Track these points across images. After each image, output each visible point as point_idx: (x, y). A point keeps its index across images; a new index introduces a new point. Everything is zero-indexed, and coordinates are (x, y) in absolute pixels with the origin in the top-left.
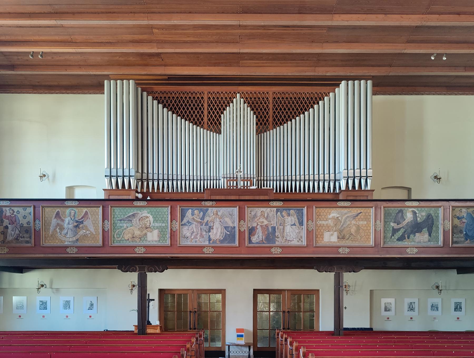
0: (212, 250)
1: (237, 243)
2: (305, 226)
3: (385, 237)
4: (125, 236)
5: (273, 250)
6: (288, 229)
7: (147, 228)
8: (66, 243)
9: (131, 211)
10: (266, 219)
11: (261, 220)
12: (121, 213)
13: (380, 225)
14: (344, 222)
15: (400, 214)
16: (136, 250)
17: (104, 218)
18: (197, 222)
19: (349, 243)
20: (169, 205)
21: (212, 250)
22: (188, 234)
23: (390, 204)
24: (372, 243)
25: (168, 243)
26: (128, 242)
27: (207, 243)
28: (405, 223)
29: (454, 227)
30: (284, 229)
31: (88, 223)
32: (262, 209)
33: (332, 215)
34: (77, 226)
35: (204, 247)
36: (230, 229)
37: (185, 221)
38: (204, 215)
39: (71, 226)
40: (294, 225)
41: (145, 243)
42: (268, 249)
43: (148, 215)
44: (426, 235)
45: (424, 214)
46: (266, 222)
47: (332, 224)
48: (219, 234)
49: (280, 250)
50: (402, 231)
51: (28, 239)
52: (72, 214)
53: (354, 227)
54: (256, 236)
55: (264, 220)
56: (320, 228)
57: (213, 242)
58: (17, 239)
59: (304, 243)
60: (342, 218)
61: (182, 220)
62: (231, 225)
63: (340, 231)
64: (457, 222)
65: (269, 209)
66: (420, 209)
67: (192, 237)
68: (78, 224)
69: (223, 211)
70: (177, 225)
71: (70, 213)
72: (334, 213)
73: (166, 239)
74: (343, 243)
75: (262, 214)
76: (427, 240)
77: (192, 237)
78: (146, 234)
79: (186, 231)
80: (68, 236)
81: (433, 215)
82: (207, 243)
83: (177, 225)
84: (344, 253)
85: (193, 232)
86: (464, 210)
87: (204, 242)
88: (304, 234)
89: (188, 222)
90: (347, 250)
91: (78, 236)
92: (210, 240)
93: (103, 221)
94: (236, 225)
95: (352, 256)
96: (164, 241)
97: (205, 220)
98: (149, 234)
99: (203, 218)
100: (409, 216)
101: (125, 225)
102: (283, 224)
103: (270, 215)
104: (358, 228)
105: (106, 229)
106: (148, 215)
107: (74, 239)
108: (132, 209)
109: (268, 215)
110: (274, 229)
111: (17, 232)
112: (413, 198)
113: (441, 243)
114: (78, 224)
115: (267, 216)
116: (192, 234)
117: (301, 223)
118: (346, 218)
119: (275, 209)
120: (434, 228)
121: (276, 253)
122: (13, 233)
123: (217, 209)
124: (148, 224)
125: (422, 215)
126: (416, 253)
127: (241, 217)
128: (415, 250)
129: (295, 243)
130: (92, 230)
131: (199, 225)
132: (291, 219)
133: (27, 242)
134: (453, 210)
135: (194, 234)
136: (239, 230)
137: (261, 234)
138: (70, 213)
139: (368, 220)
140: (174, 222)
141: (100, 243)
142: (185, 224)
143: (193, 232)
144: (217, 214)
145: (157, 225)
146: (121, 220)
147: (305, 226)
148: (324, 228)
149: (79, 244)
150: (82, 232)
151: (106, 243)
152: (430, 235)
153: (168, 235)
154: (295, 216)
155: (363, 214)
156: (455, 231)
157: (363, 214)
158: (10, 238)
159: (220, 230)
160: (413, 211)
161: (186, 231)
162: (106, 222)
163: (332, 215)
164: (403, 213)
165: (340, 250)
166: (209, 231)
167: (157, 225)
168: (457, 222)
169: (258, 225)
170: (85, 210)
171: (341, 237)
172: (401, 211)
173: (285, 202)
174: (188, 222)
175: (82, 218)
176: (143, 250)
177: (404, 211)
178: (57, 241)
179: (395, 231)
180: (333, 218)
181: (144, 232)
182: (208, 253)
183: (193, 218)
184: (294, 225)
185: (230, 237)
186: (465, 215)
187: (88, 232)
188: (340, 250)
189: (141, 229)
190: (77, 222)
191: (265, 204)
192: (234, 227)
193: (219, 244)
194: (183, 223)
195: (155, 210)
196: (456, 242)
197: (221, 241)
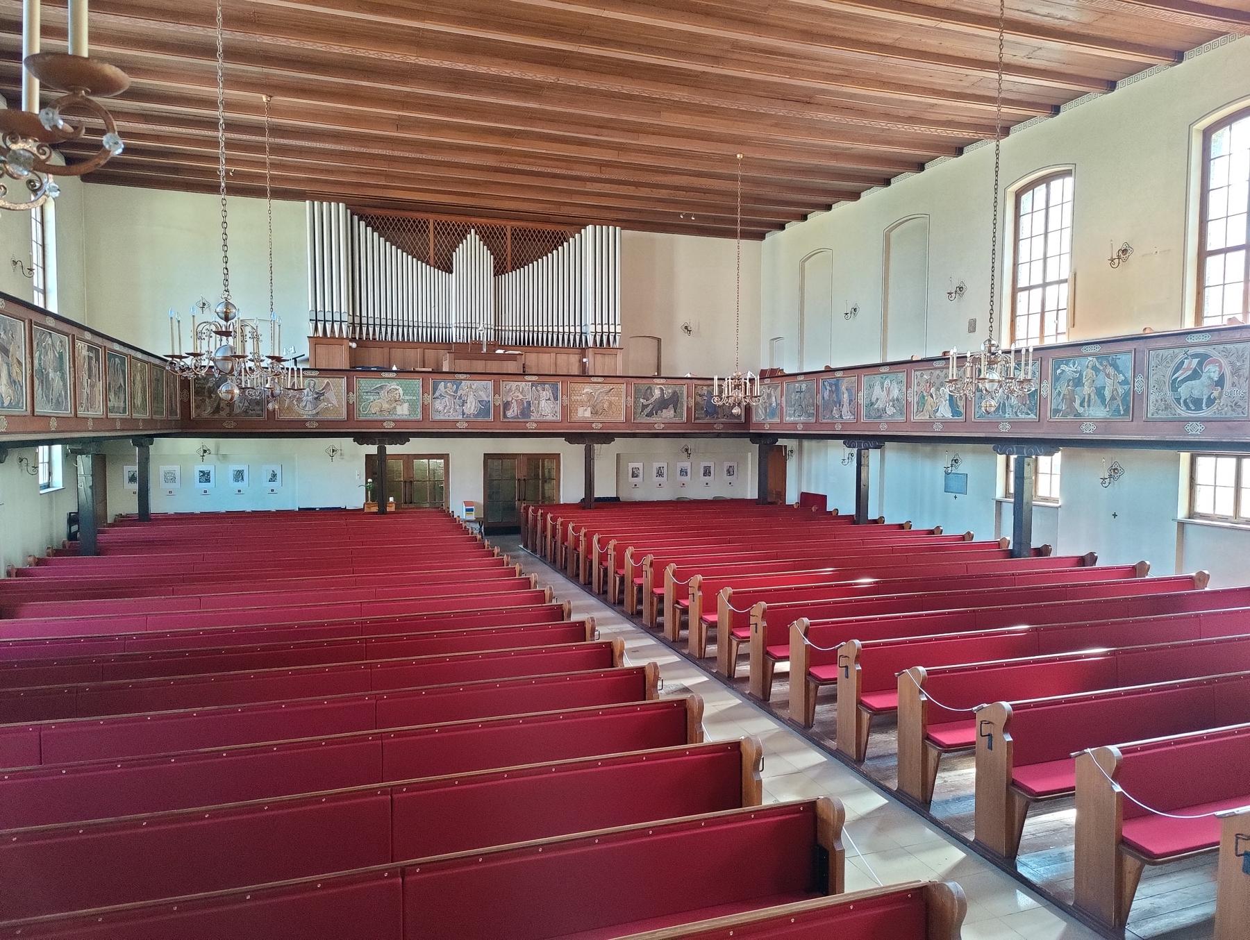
0: (466, 425)
1: (491, 418)
2: (559, 402)
3: (634, 413)
4: (372, 409)
5: (528, 425)
6: (543, 403)
7: (396, 401)
8: (305, 417)
9: (378, 383)
10: (521, 393)
11: (516, 394)
12: (367, 385)
13: (631, 401)
14: (597, 398)
15: (649, 391)
16: (385, 424)
17: (350, 388)
18: (450, 395)
19: (602, 418)
20: (421, 376)
21: (466, 425)
22: (441, 408)
23: (640, 381)
24: (623, 419)
25: (419, 417)
26: (375, 415)
27: (461, 417)
28: (653, 400)
29: (696, 404)
30: (539, 404)
31: (330, 395)
32: (517, 383)
33: (585, 391)
34: (316, 398)
35: (458, 422)
36: (484, 403)
37: (437, 394)
38: (457, 388)
39: (310, 398)
40: (549, 399)
41: (394, 417)
42: (523, 424)
43: (398, 387)
44: (672, 412)
45: (670, 391)
46: (521, 397)
47: (586, 399)
48: (473, 408)
49: (535, 425)
50: (651, 406)
51: (260, 412)
52: (312, 385)
53: (607, 403)
54: (511, 411)
55: (519, 394)
56: (575, 403)
57: (467, 417)
58: (246, 412)
59: (559, 418)
60: (595, 394)
61: (434, 394)
62: (486, 399)
63: (594, 407)
64: (699, 399)
65: (524, 383)
66: (666, 386)
67: (445, 411)
68: (319, 396)
69: (476, 384)
70: (428, 398)
71: (309, 384)
72: (587, 389)
73: (417, 412)
74: (596, 418)
75: (517, 388)
76: (673, 416)
77: (445, 411)
78: (395, 408)
79: (438, 405)
80: (306, 409)
81: (678, 392)
82: (461, 417)
83: (428, 398)
84: (597, 428)
85: (446, 406)
86: (705, 388)
87: (458, 416)
88: (559, 409)
89: (441, 395)
90: (600, 425)
91: (318, 410)
92: (463, 414)
93: (348, 393)
94: (491, 399)
95: (605, 431)
96: (415, 416)
97: (459, 394)
98: (398, 408)
99: (456, 392)
100: (657, 393)
101: (372, 398)
102: (538, 398)
103: (525, 389)
104: (611, 403)
105: (351, 402)
106: (398, 387)
107: (314, 412)
108: (380, 381)
109: (523, 388)
110: (529, 403)
111: (246, 404)
112: (662, 376)
113: (685, 419)
114: (319, 396)
115: (522, 391)
116: (444, 408)
117: (556, 399)
118: (599, 394)
119: (530, 383)
120: (679, 405)
121: (531, 427)
122: (241, 405)
123: (471, 382)
124: (397, 397)
125: (668, 392)
126: (663, 429)
127: (497, 391)
128: (663, 426)
129: (550, 418)
130: (335, 402)
131: (452, 399)
132: (546, 394)
133: (259, 415)
134: (695, 387)
135: (447, 408)
136: (494, 404)
137: (516, 409)
138: (309, 384)
139: (618, 395)
140: (426, 395)
141: (344, 416)
142: (437, 398)
143: (446, 406)
144: (471, 387)
145: (407, 398)
146: (367, 392)
147: (559, 402)
148: (578, 403)
149: (319, 417)
150: (323, 405)
151: (351, 416)
152: (675, 412)
153: (419, 410)
154: (550, 391)
155: (616, 390)
156: (697, 408)
157: (616, 390)
158: (237, 411)
159: (474, 404)
160: (660, 388)
161: (438, 405)
162: (351, 394)
163: (585, 391)
164: (651, 389)
165: (594, 425)
166: (463, 405)
167: (407, 398)
168: (699, 399)
169: (513, 399)
170: (326, 381)
171: (594, 413)
172: (650, 388)
173: (541, 377)
174: (441, 395)
175: (323, 390)
176: (393, 424)
177: (653, 388)
178: (294, 415)
179: (645, 407)
180: (587, 393)
181: (393, 406)
182: (462, 427)
183: (446, 392)
184: (549, 399)
185: (484, 409)
186: (706, 393)
187: (329, 405)
188: (594, 425)
189: (389, 402)
190: (317, 393)
191: (520, 378)
192: (489, 401)
193: (472, 419)
194: (435, 396)
195: (405, 382)
196: (698, 418)
197: (476, 416)
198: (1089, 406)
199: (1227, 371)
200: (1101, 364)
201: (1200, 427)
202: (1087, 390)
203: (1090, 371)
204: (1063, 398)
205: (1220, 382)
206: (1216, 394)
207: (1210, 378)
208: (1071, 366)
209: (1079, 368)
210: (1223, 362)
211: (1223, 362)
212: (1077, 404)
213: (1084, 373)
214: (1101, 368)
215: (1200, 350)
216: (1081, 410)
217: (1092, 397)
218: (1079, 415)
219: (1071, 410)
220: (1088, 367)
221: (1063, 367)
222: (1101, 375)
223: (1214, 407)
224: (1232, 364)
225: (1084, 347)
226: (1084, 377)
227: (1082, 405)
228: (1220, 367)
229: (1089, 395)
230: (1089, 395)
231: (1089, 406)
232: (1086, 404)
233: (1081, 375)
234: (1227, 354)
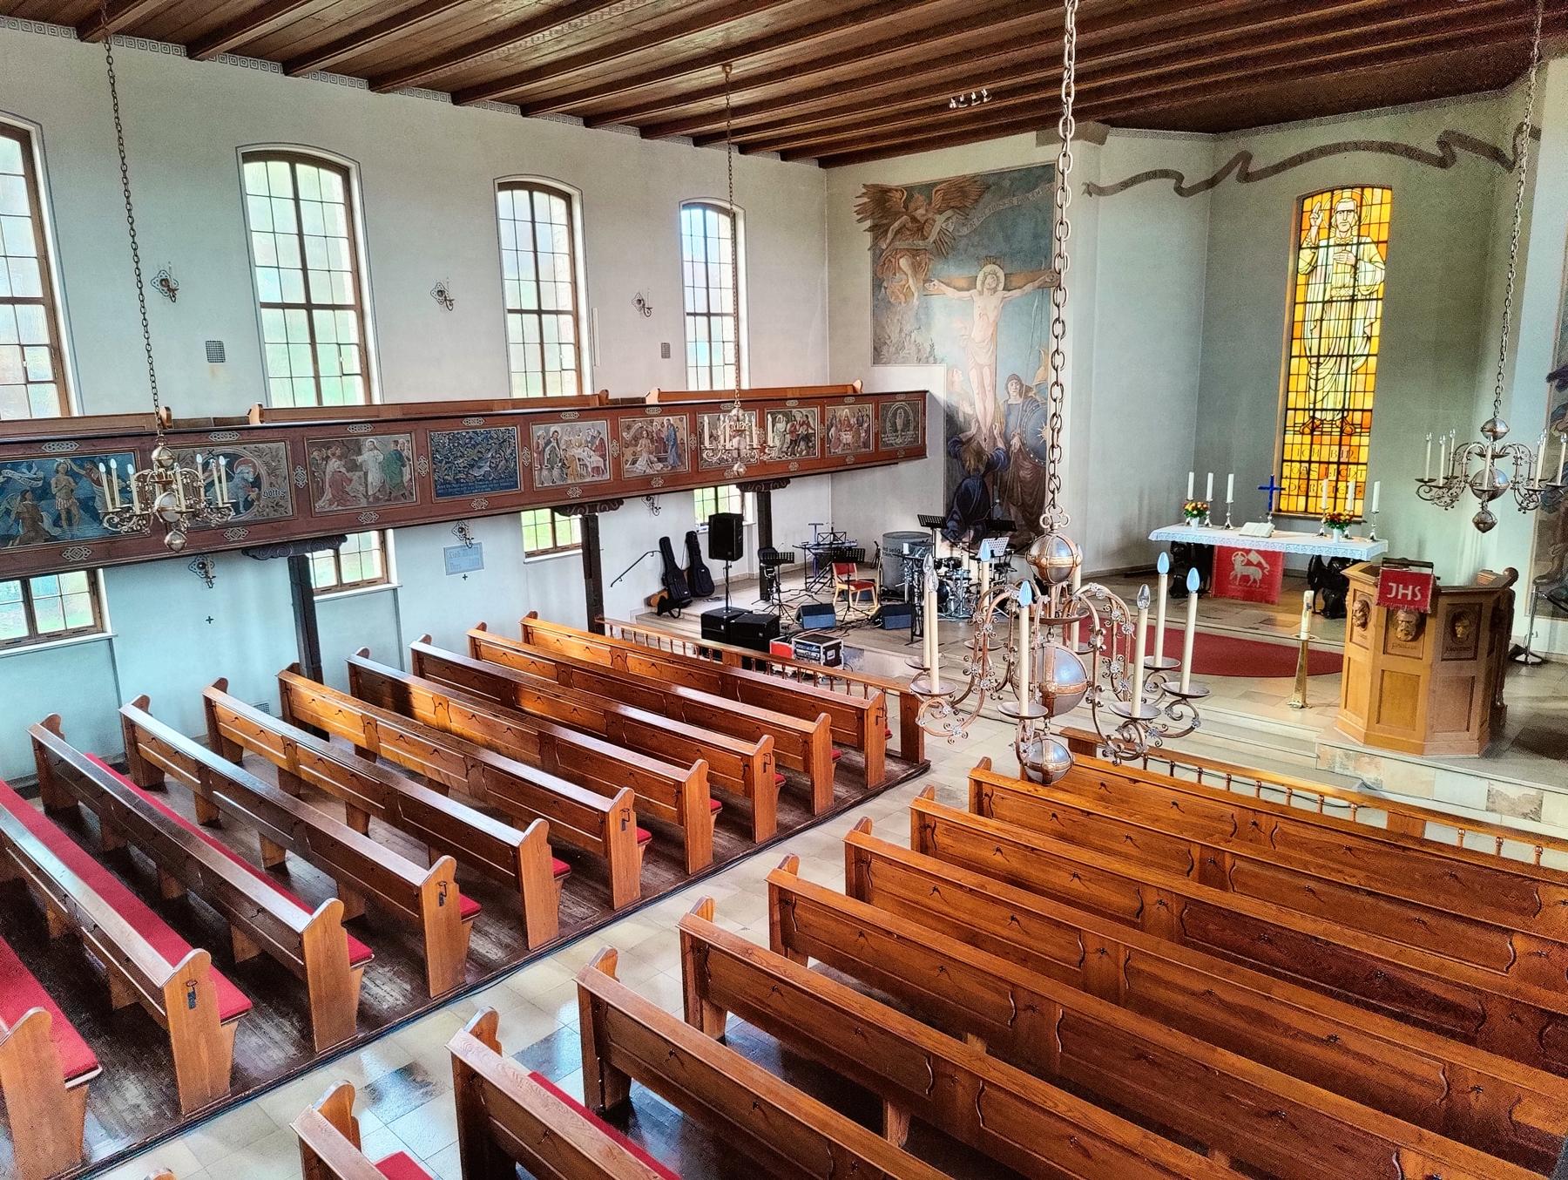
198: (70, 524)
199: (263, 471)
200: (82, 467)
201: (242, 532)
202: (61, 503)
203: (61, 477)
204: (16, 521)
205: (257, 483)
206: (253, 495)
207: (243, 479)
208: (25, 470)
209: (41, 474)
210: (257, 462)
211: (257, 462)
212: (47, 524)
213: (53, 481)
214: (83, 472)
215: (229, 450)
216: (56, 532)
217: (74, 511)
218: (55, 538)
219: (37, 532)
220: (57, 472)
221: (8, 473)
222: (85, 483)
223: (254, 509)
224: (266, 464)
225: (46, 444)
226: (53, 485)
227: (56, 523)
228: (254, 466)
229: (68, 511)
230: (68, 511)
231: (70, 524)
232: (64, 523)
233: (47, 485)
234: (260, 455)
